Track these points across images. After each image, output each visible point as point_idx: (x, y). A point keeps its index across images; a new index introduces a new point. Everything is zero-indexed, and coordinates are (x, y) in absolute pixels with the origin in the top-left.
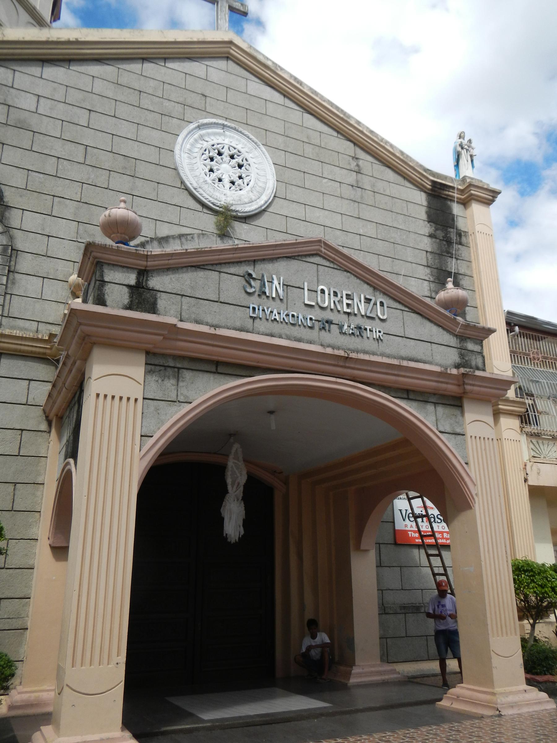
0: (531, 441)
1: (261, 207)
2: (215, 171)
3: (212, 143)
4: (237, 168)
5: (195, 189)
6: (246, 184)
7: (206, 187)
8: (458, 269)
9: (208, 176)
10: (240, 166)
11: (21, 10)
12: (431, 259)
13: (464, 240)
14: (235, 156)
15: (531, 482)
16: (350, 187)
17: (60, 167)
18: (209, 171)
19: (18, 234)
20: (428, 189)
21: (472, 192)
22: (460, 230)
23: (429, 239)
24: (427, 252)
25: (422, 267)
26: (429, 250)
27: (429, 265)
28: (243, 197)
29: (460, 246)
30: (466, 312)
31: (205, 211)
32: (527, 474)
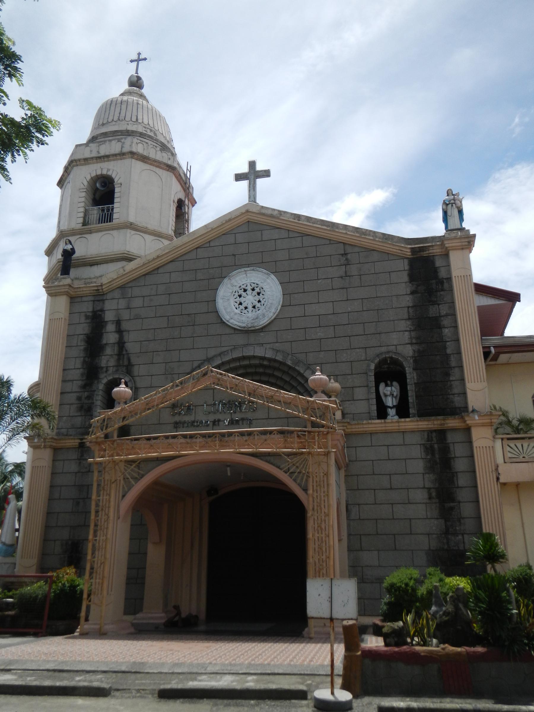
0: (508, 445)
1: (271, 318)
2: (243, 303)
3: (239, 286)
4: (257, 295)
5: (228, 321)
6: (262, 305)
7: (236, 317)
8: (440, 313)
9: (238, 308)
10: (259, 294)
11: (147, 236)
12: (413, 312)
13: (446, 285)
14: (255, 288)
15: (502, 480)
16: (340, 278)
17: (156, 334)
18: (239, 305)
19: (137, 379)
20: (409, 255)
21: (447, 245)
22: (443, 278)
23: (411, 296)
24: (408, 307)
25: (403, 322)
26: (411, 305)
27: (410, 317)
28: (259, 315)
29: (442, 293)
30: (447, 346)
31: (236, 332)
32: (499, 474)
